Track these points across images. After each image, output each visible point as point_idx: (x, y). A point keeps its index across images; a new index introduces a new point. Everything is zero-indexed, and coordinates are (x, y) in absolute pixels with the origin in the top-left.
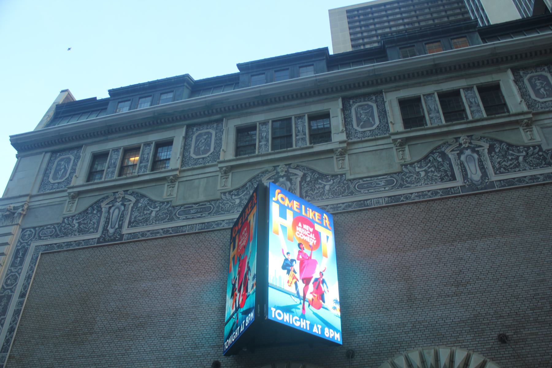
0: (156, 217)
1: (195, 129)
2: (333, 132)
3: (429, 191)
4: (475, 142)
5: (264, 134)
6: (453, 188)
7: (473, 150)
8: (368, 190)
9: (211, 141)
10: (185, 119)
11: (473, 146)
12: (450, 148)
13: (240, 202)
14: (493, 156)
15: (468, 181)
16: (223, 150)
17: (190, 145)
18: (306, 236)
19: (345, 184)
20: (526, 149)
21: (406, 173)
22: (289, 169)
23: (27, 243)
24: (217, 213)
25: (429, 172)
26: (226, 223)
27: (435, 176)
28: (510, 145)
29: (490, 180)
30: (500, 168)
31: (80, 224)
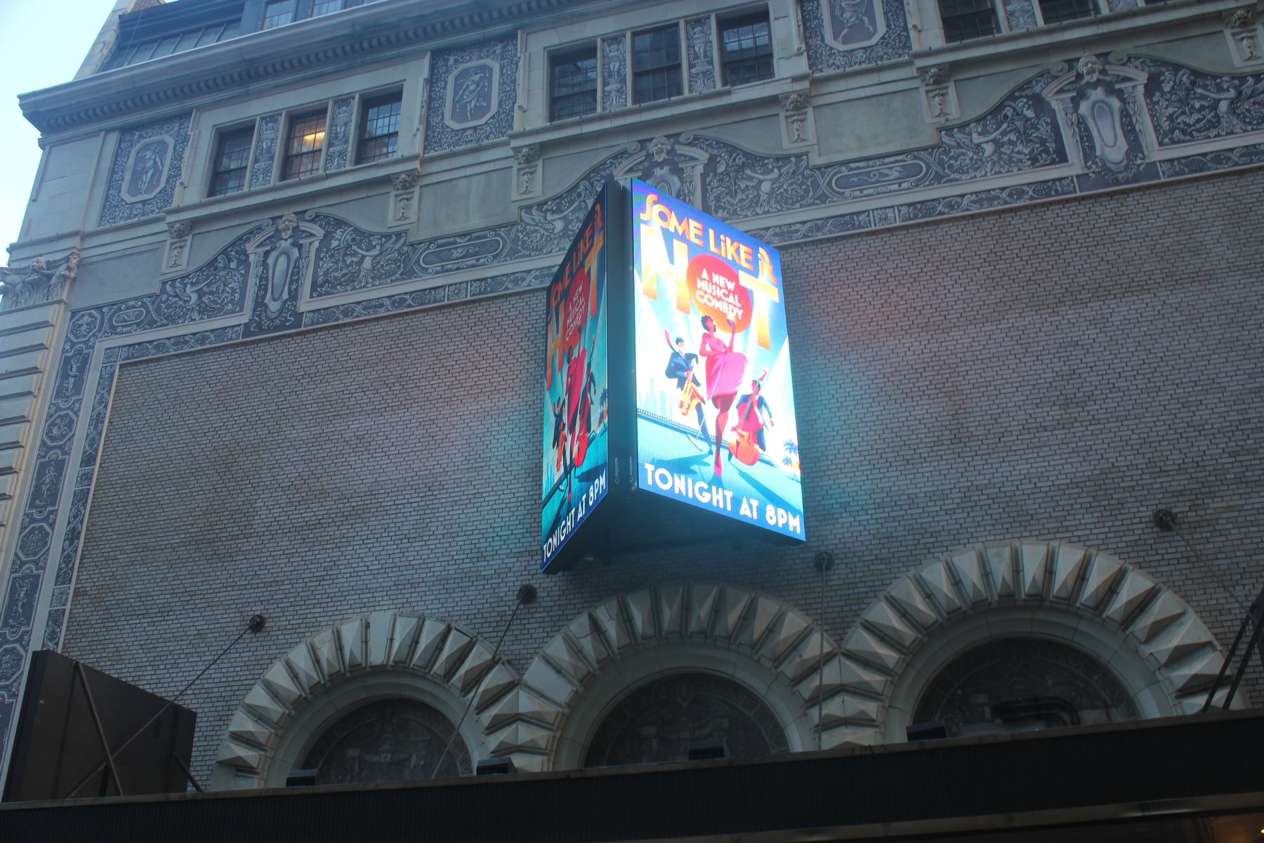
0: (374, 269)
1: (452, 59)
2: (777, 53)
3: (1003, 189)
4: (1113, 70)
5: (615, 66)
6: (1060, 180)
7: (1110, 90)
8: (861, 191)
9: (490, 87)
11: (1108, 78)
12: (1056, 85)
13: (566, 228)
14: (1157, 103)
15: (1096, 164)
16: (520, 107)
17: (441, 98)
18: (719, 299)
19: (807, 178)
20: (1236, 82)
21: (951, 147)
22: (677, 147)
23: (84, 342)
24: (514, 254)
25: (1004, 144)
26: (536, 278)
27: (1019, 152)
28: (1197, 74)
29: (1147, 161)
30: (1172, 131)
31: (200, 293)
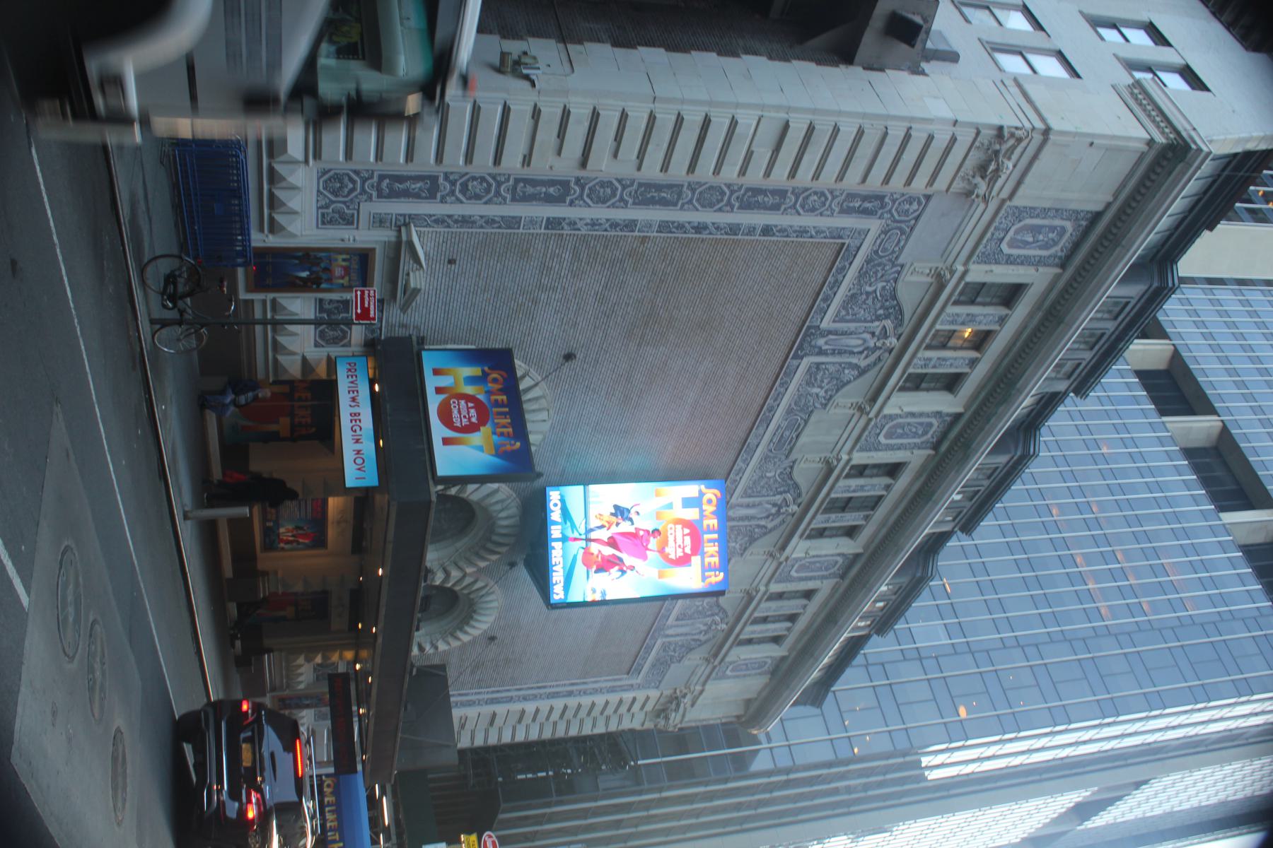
10: (970, 422)
